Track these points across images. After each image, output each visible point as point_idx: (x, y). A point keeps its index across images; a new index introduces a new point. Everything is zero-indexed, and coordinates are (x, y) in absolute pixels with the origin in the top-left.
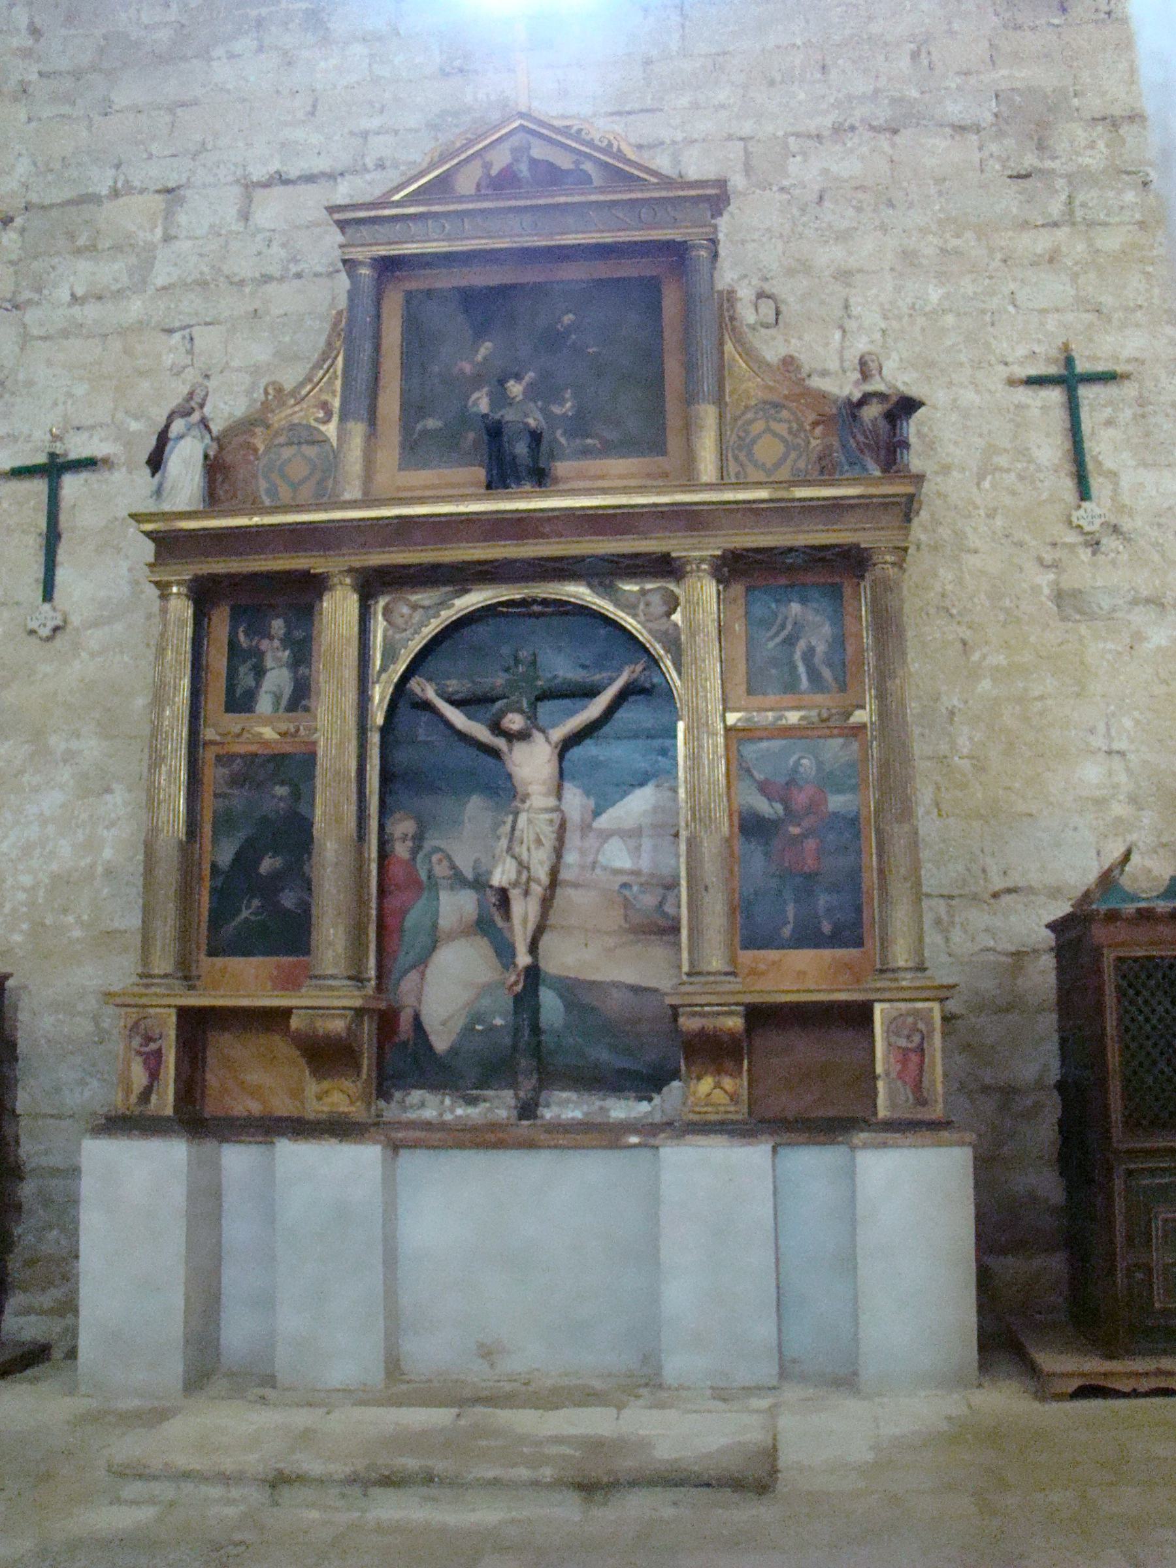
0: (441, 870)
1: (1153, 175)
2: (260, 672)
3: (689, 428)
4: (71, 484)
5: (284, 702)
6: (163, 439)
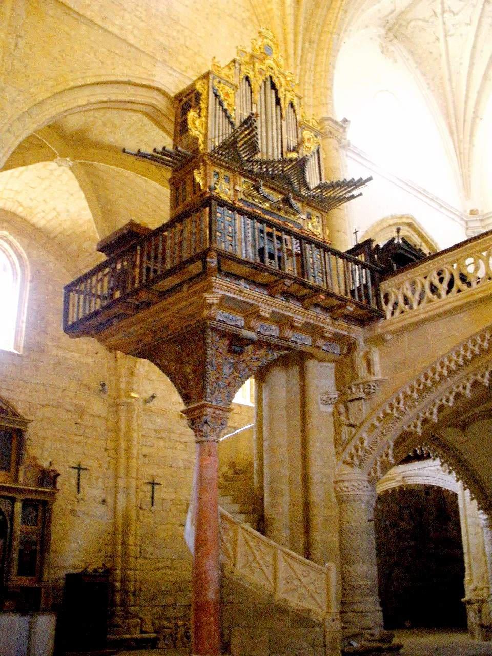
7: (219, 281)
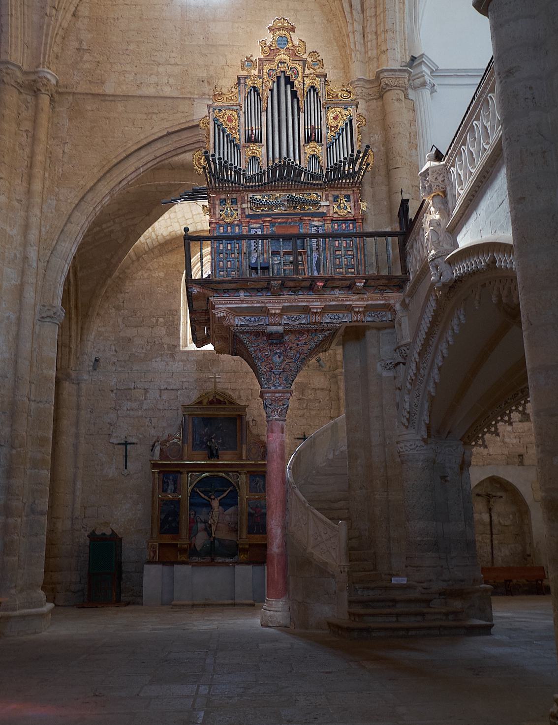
0: (199, 520)
1: (322, 400)
2: (168, 485)
3: (241, 448)
4: (129, 447)
5: (173, 491)
6: (153, 446)
7: (216, 299)
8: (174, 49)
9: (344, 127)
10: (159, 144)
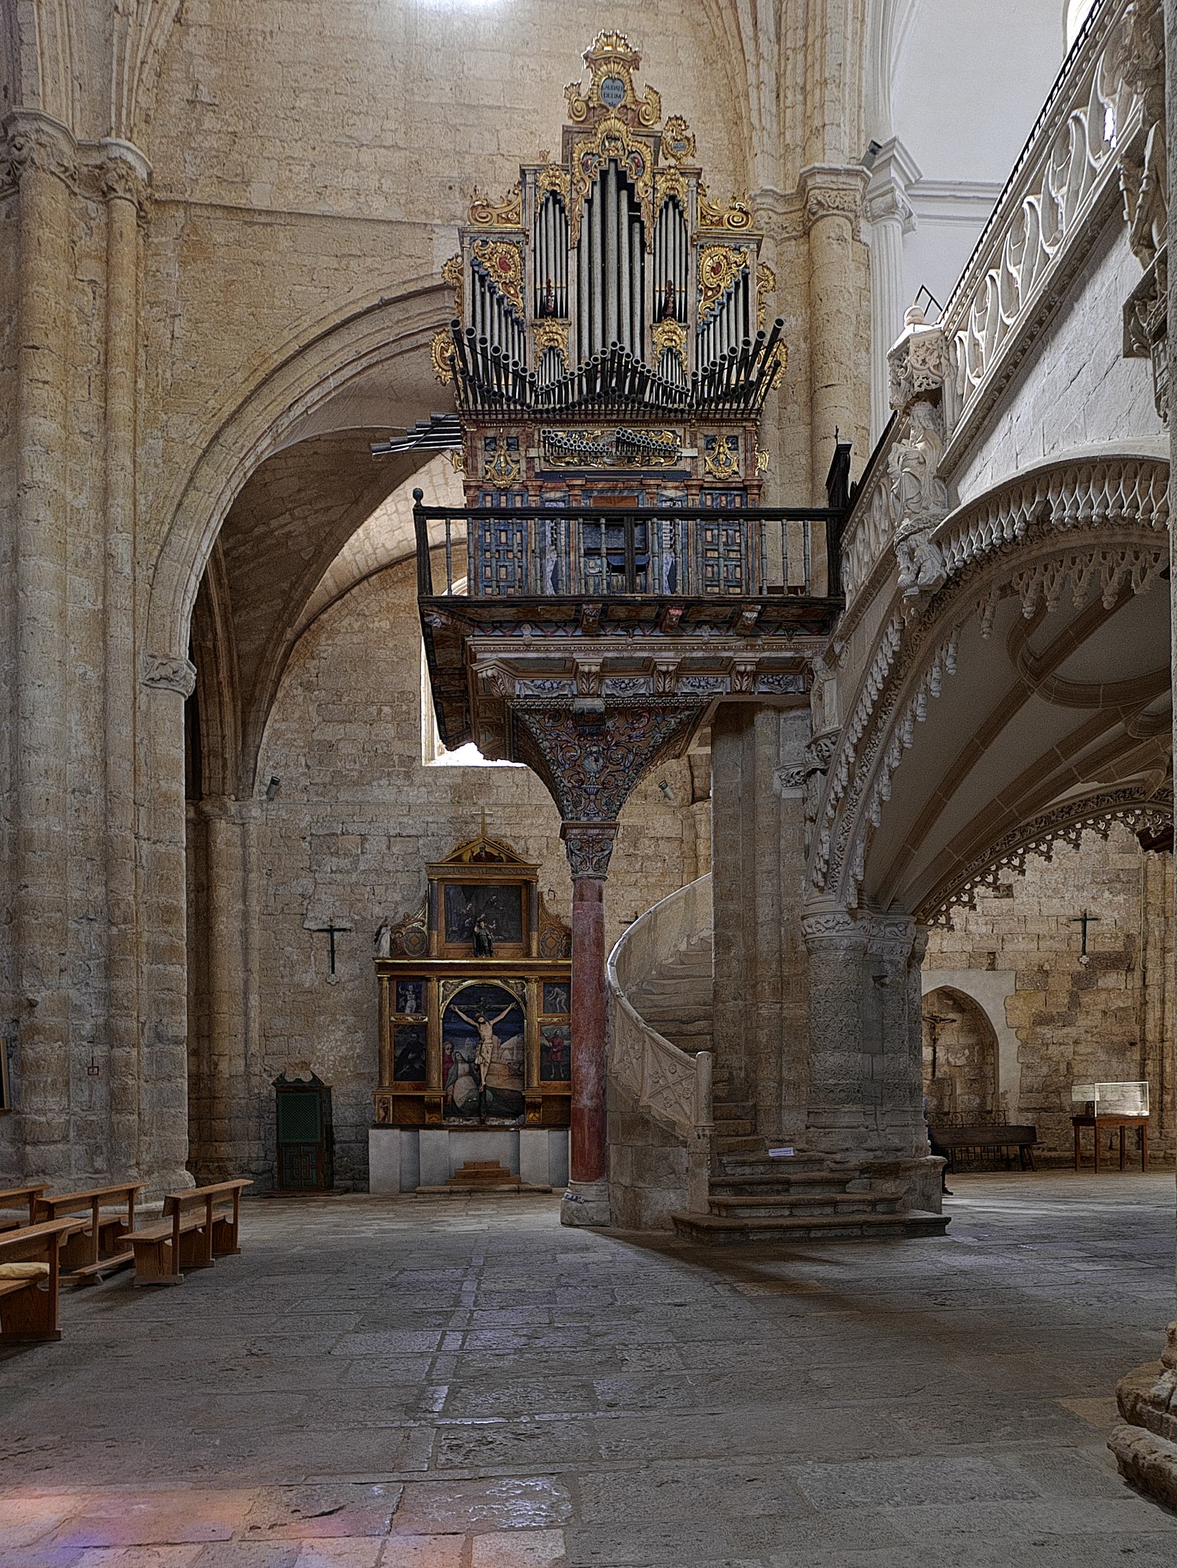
0: (459, 1058)
2: (406, 1001)
3: (529, 938)
4: (337, 935)
8: (392, 112)
9: (733, 290)
10: (363, 327)
